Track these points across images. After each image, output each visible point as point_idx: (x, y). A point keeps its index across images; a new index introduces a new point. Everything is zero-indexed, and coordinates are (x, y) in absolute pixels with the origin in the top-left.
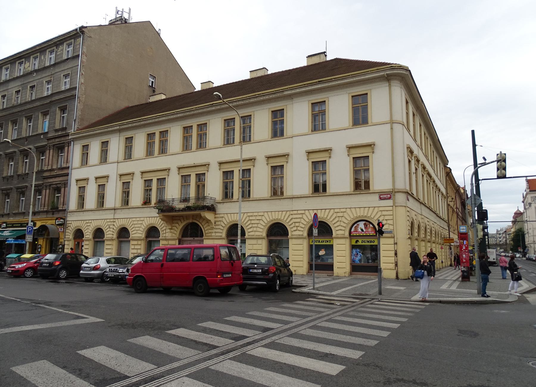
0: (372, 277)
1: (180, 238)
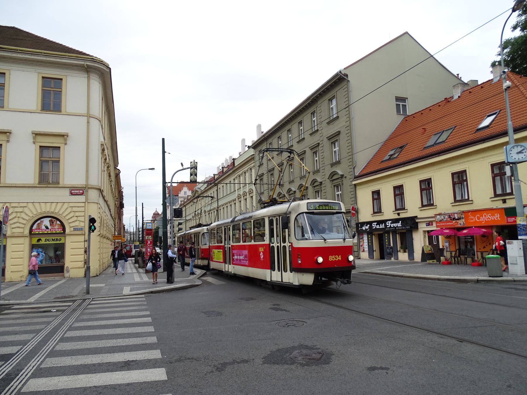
0: (57, 278)
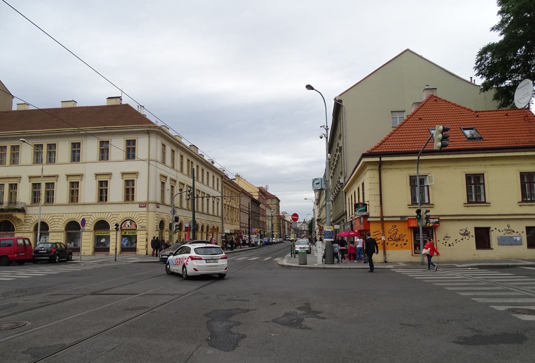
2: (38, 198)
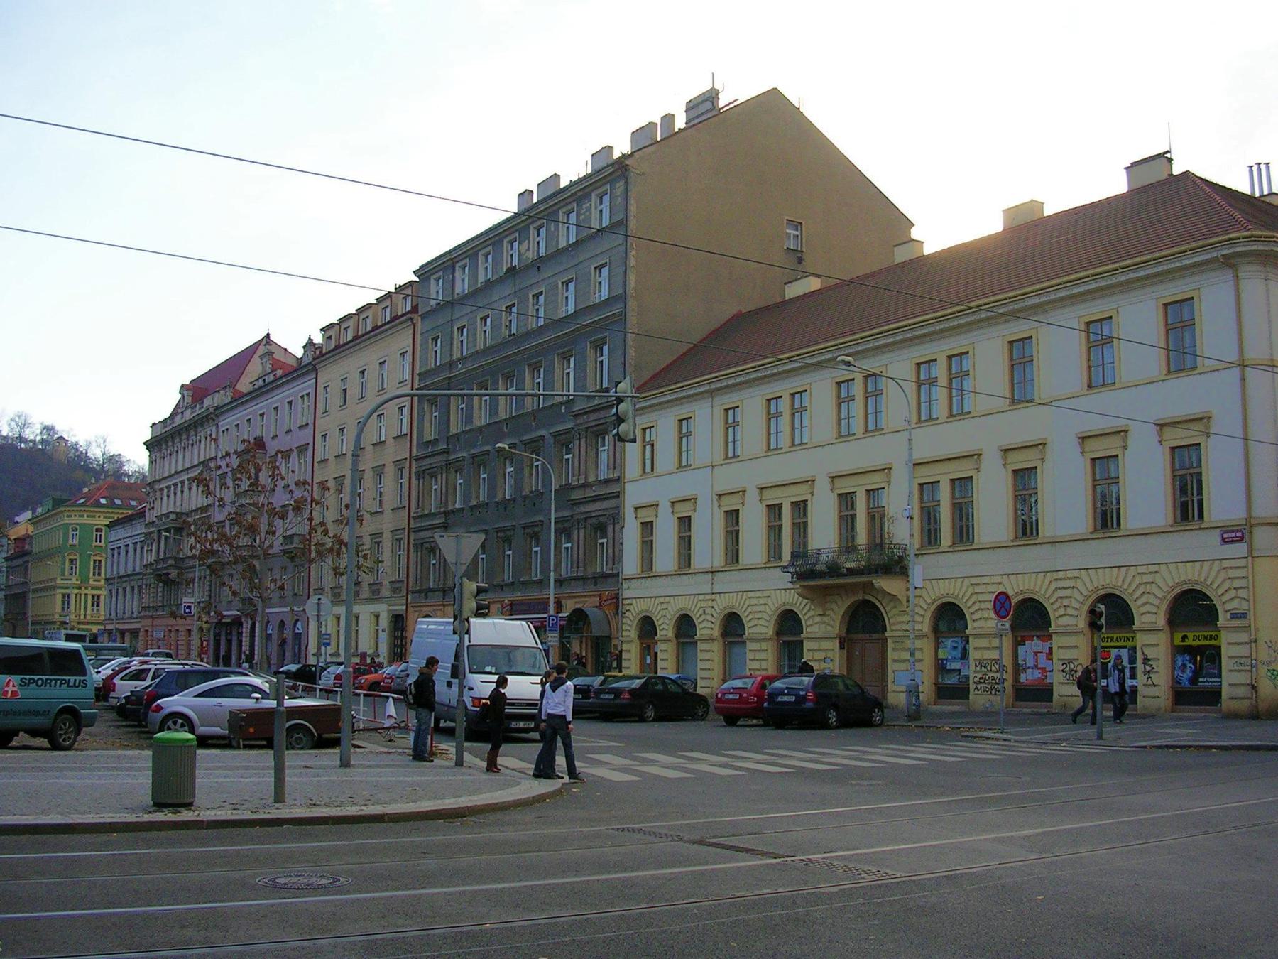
1: (844, 635)
2: (968, 526)
